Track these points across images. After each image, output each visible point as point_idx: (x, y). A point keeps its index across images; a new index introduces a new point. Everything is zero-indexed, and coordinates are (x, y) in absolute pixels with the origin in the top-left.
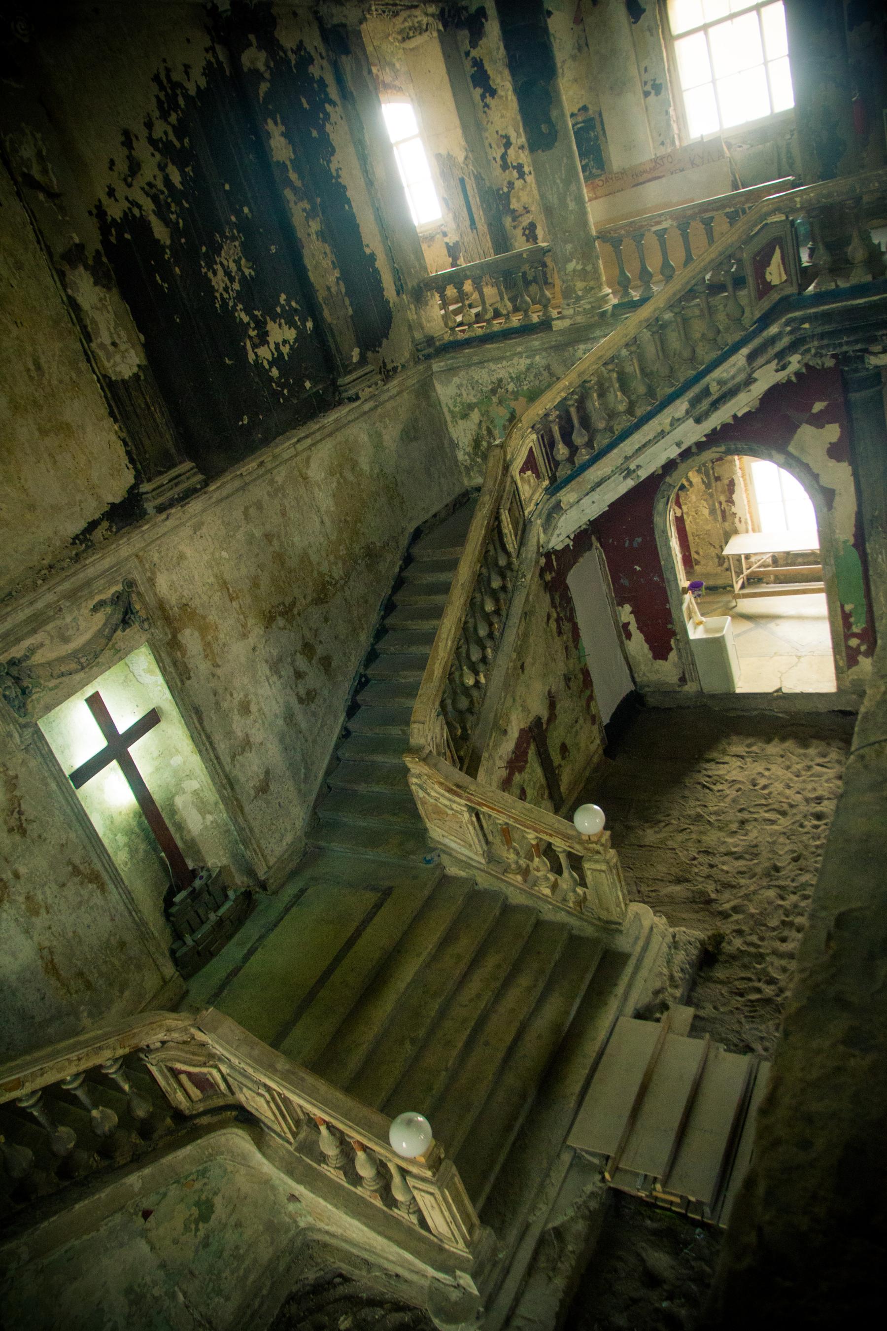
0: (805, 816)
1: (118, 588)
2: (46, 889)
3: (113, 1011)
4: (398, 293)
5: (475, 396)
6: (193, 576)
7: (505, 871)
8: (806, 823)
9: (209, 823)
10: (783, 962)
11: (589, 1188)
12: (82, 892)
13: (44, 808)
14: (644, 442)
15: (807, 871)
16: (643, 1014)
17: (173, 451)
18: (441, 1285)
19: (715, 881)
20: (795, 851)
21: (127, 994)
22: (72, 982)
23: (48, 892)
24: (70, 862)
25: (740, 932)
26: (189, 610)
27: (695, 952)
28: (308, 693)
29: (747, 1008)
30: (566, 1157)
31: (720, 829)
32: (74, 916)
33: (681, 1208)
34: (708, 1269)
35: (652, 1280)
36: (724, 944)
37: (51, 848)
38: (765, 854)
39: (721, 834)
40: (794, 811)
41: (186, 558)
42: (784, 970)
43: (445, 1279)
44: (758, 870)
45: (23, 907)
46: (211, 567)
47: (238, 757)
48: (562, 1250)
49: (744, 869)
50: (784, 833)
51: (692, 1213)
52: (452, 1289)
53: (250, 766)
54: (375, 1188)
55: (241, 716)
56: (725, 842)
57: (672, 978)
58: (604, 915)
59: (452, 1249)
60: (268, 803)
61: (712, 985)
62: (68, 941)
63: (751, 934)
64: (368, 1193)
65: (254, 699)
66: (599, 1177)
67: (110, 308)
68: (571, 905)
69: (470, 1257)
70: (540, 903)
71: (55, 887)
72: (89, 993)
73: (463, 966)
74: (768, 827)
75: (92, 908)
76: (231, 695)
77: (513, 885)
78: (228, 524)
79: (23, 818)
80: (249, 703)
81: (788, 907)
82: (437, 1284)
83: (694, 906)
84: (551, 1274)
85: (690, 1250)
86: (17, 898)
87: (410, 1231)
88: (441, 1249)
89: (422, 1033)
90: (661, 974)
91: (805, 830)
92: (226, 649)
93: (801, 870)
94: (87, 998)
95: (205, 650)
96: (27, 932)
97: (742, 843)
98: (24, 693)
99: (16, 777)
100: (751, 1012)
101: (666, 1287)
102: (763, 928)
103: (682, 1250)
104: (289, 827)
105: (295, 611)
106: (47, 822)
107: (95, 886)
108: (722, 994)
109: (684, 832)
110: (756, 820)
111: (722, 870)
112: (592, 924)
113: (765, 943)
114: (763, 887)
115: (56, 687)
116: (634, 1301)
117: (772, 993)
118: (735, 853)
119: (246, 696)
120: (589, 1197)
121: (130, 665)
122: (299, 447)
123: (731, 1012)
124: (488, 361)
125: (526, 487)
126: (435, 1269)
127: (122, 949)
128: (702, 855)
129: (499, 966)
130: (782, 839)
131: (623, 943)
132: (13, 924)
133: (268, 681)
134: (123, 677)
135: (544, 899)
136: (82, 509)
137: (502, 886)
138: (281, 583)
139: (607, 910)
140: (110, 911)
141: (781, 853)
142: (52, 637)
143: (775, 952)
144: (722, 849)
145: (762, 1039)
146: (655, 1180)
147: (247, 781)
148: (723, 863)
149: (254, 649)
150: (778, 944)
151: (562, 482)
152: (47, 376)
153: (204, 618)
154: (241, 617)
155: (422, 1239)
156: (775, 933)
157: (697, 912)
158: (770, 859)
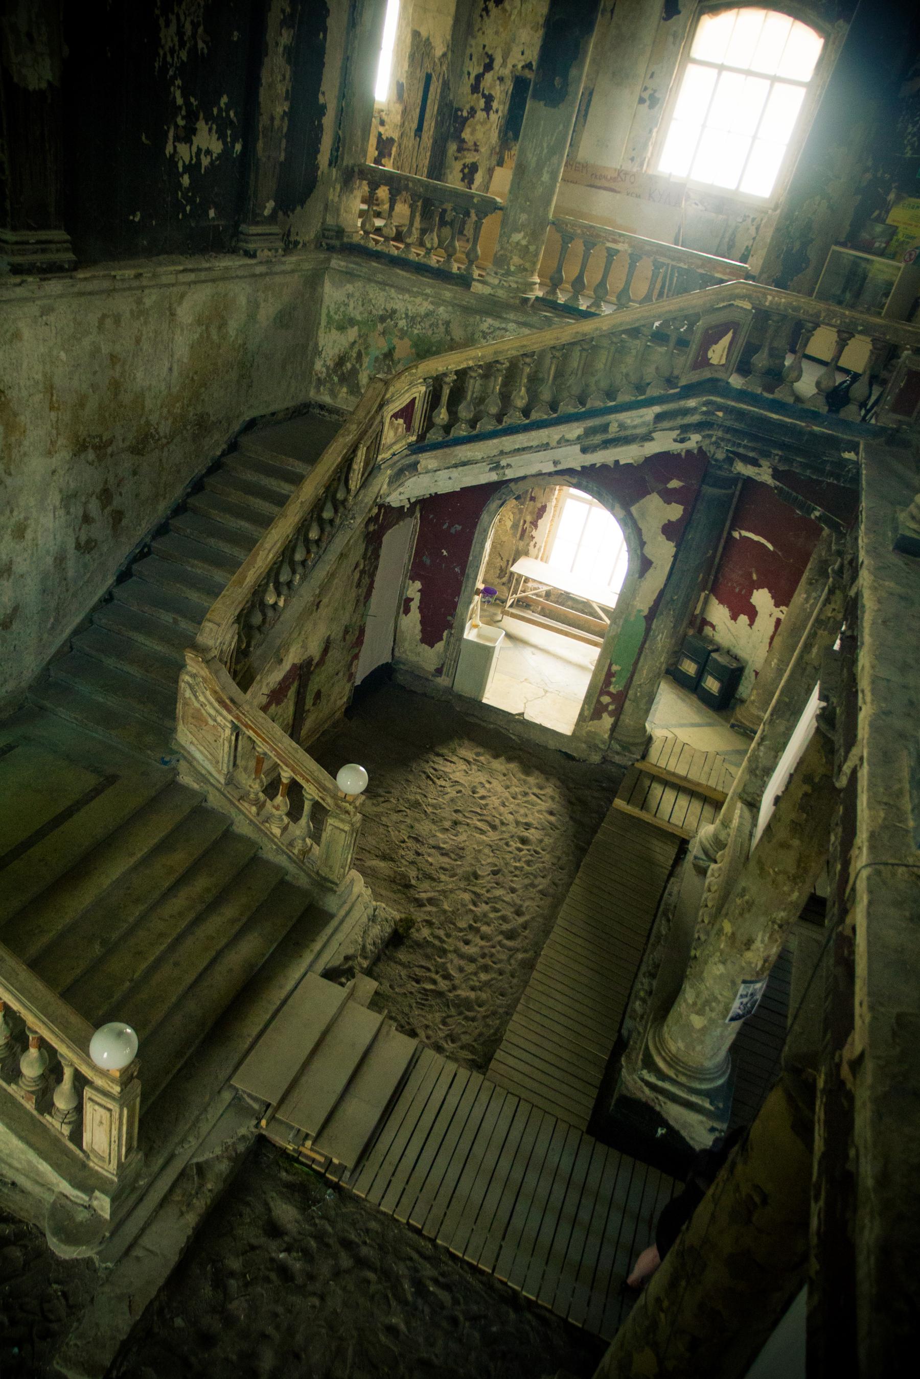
0: (512, 837)
4: (330, 165)
5: (361, 313)
6: (21, 365)
7: (241, 798)
8: (512, 843)
10: (462, 963)
11: (243, 1131)
14: (526, 445)
15: (502, 887)
16: (332, 974)
18: (68, 1202)
19: (418, 870)
20: (496, 865)
25: (429, 923)
26: (3, 399)
27: (389, 930)
28: (88, 542)
29: (420, 996)
30: (227, 1096)
31: (434, 822)
33: (321, 1167)
34: (330, 1229)
35: (274, 1230)
36: (413, 930)
38: (469, 859)
39: (434, 827)
40: (504, 829)
41: (21, 340)
42: (461, 970)
43: (77, 1197)
44: (459, 871)
46: (44, 363)
48: (201, 1186)
49: (447, 866)
50: (491, 846)
51: (330, 1174)
52: (81, 1209)
54: (33, 1089)
56: (435, 836)
57: (364, 947)
58: (324, 872)
59: (97, 1168)
61: (392, 964)
63: (439, 928)
64: (23, 1093)
66: (254, 1122)
68: (296, 851)
69: (116, 1179)
70: (265, 840)
73: (172, 879)
74: (477, 835)
76: (12, 511)
77: (244, 814)
80: (26, 528)
81: (479, 914)
82: (64, 1201)
83: (393, 885)
84: (184, 1209)
85: (320, 1209)
87: (56, 1141)
88: (84, 1166)
89: (115, 936)
90: (357, 942)
91: (510, 849)
93: (497, 884)
97: (451, 842)
100: (422, 999)
101: (286, 1238)
102: (452, 926)
103: (309, 1207)
105: (109, 450)
108: (400, 976)
109: (400, 814)
110: (468, 825)
111: (427, 861)
112: (309, 876)
113: (450, 940)
114: (460, 889)
116: (253, 1248)
117: (446, 988)
118: (443, 848)
119: (26, 519)
120: (239, 1139)
122: (182, 278)
123: (405, 994)
124: (392, 286)
125: (392, 433)
126: (73, 1186)
128: (411, 840)
129: (208, 890)
130: (487, 851)
131: (331, 903)
135: (271, 838)
137: (233, 812)
138: (107, 415)
139: (331, 867)
141: (483, 862)
143: (456, 951)
144: (431, 841)
145: (427, 1027)
146: (307, 1136)
148: (429, 855)
149: (54, 472)
150: (461, 945)
151: (428, 445)
154: (54, 432)
155: (67, 1152)
156: (461, 934)
157: (394, 892)
158: (472, 865)
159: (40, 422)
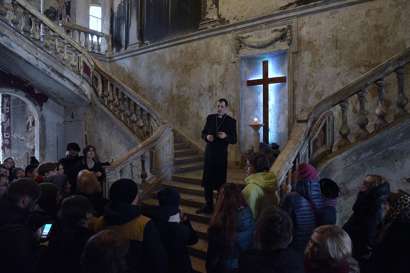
1: (285, 27)
26: (312, 45)
45: (214, 103)
55: (315, 97)
65: (326, 94)
76: (315, 86)
92: (323, 67)
95: (311, 63)
98: (240, 46)
99: (228, 69)
107: (232, 114)
115: (250, 50)
119: (322, 91)
142: (256, 34)
149: (338, 74)
153: (318, 50)
154: (339, 58)
159: (330, 53)
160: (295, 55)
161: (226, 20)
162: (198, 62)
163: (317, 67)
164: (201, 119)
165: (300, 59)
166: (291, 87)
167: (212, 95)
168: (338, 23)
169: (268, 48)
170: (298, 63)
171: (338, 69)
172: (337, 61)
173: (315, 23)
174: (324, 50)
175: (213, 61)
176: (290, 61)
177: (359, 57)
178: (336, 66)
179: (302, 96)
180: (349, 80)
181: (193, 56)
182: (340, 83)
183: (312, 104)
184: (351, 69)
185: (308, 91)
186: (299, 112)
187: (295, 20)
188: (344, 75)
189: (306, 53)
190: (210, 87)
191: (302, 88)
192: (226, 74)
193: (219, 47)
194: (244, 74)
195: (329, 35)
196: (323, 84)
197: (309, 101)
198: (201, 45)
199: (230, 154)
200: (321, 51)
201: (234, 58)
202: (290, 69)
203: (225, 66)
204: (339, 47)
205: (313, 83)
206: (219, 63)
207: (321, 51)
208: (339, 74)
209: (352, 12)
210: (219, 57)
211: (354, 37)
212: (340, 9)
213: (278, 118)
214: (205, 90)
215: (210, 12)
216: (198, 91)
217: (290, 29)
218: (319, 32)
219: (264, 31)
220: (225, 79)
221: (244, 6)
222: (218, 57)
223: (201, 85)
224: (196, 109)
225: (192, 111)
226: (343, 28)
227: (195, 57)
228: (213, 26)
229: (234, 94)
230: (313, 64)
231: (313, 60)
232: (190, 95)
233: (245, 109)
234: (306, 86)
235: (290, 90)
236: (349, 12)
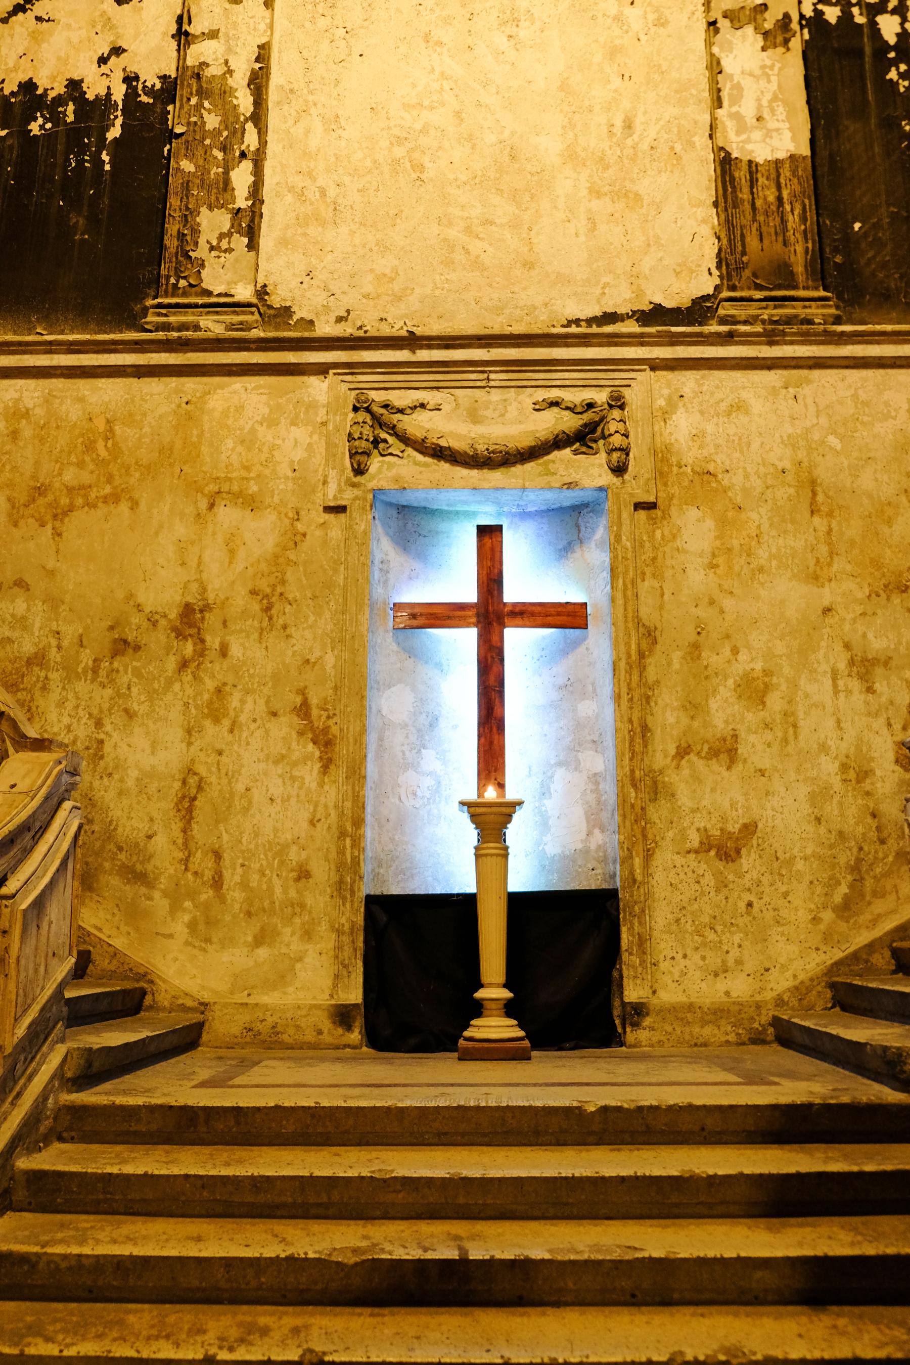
1: (601, 397)
2: (250, 699)
3: (226, 957)
6: (749, 445)
9: (593, 846)
12: (294, 745)
13: (314, 598)
17: (799, 269)
21: (263, 953)
22: (199, 854)
23: (249, 706)
24: (302, 692)
26: (714, 485)
32: (262, 766)
37: (290, 653)
41: (747, 413)
45: (206, 696)
46: (795, 447)
47: (693, 757)
53: (713, 790)
60: (722, 885)
62: (232, 794)
65: (784, 687)
67: (774, 79)
71: (262, 707)
72: (211, 892)
75: (293, 779)
76: (735, 651)
78: (866, 404)
79: (279, 589)
86: (206, 679)
94: (204, 897)
95: (714, 555)
96: (189, 732)
99: (304, 535)
104: (749, 967)
106: (306, 617)
115: (426, 465)
119: (767, 673)
121: (583, 529)
127: (298, 879)
132: (179, 706)
133: (834, 680)
134: (565, 542)
136: (604, 293)
140: (316, 806)
147: (695, 810)
149: (827, 610)
152: (635, 137)
154: (824, 549)
159: (790, 527)
160: (642, 514)
161: (296, 317)
162: (117, 481)
163: (739, 575)
164: (116, 777)
165: (666, 533)
166: (628, 644)
167: (201, 653)
168: (815, 421)
169: (518, 469)
170: (655, 548)
171: (826, 591)
172: (818, 559)
173: (723, 406)
174: (763, 511)
175: (212, 488)
176: (624, 538)
177: (900, 555)
178: (816, 579)
179: (679, 689)
180: (870, 636)
181: (90, 447)
182: (838, 647)
183: (726, 722)
184: (873, 595)
185: (706, 667)
186: (669, 759)
187: (645, 376)
188: (851, 615)
189: (693, 513)
190: (188, 611)
191: (677, 657)
192: (292, 557)
193: (253, 430)
194: (381, 570)
195: (781, 459)
196: (770, 645)
197: (713, 711)
198: (146, 401)
199: (298, 966)
200: (754, 515)
201: (340, 491)
202: (621, 569)
203: (287, 521)
204: (824, 509)
205: (728, 636)
206: (252, 503)
207: (754, 515)
208: (829, 610)
209: (860, 392)
210: (252, 475)
211: (876, 480)
212: (816, 373)
213: (542, 785)
214: (155, 624)
215: (212, 260)
216: (112, 628)
217: (622, 407)
218: (740, 439)
219: (496, 396)
220: (283, 582)
221: (392, 280)
222: (244, 474)
223: (130, 596)
224: (84, 720)
225: (56, 730)
226: (833, 441)
227: (103, 453)
228: (231, 327)
229: (330, 660)
230: (720, 560)
231: (723, 544)
232: (54, 642)
233: (381, 739)
234: (696, 647)
235: (623, 656)
236: (852, 391)
